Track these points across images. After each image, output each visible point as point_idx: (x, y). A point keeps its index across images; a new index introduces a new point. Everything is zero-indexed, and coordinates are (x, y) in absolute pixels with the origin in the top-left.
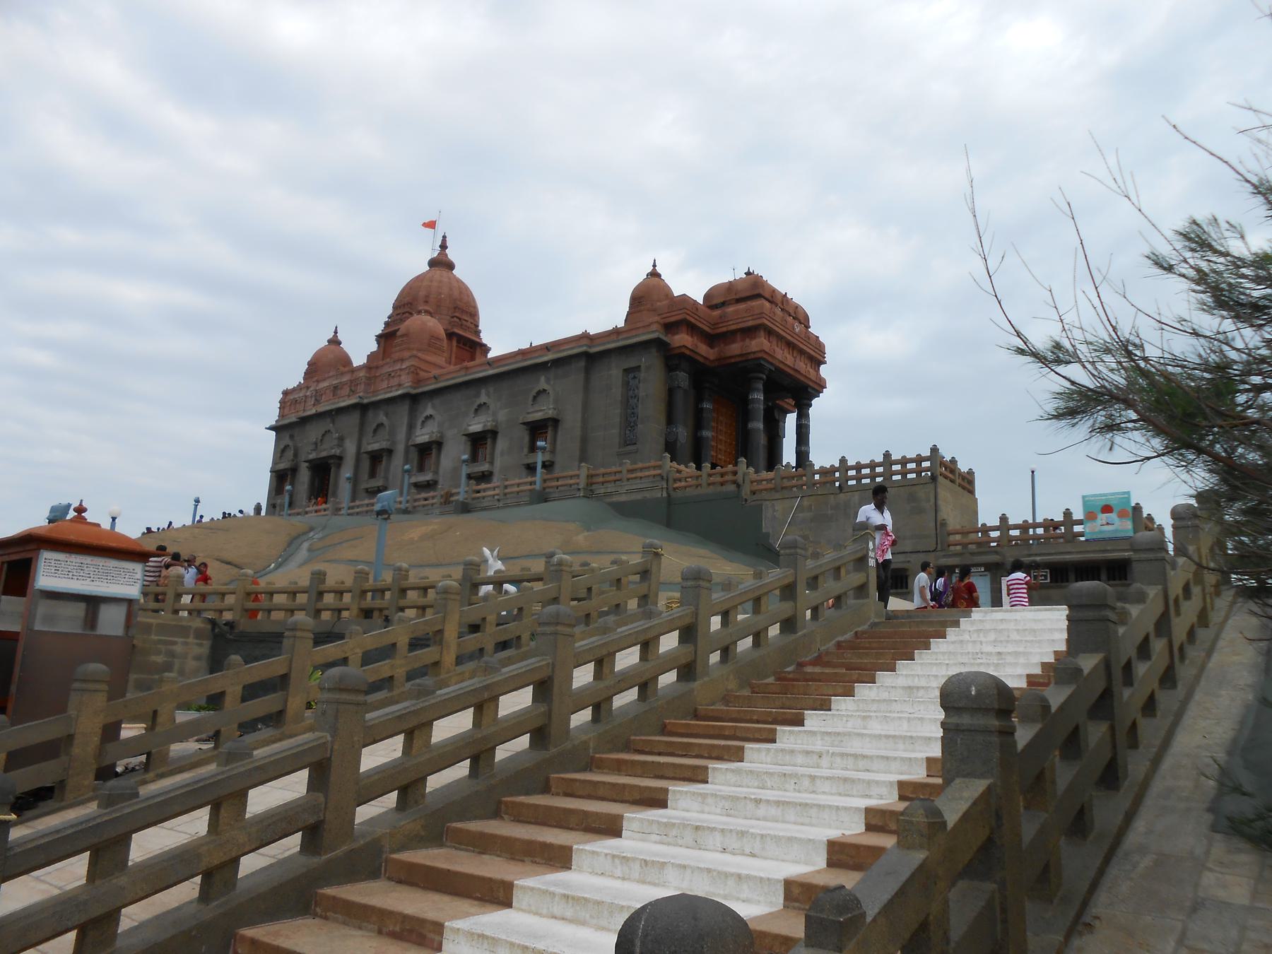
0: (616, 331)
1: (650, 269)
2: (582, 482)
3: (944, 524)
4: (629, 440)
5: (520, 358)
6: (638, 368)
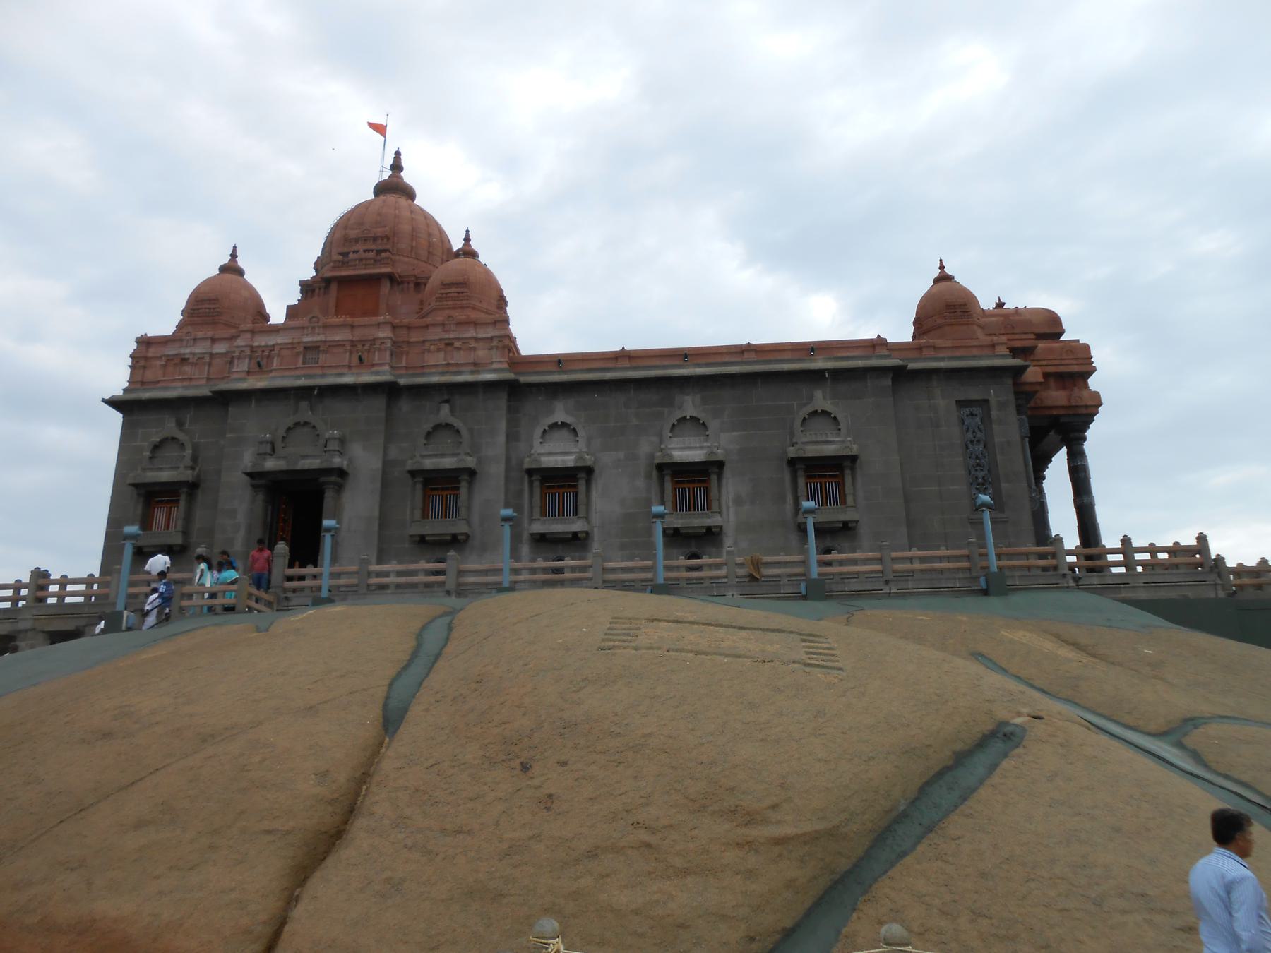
5: (753, 357)
6: (985, 403)
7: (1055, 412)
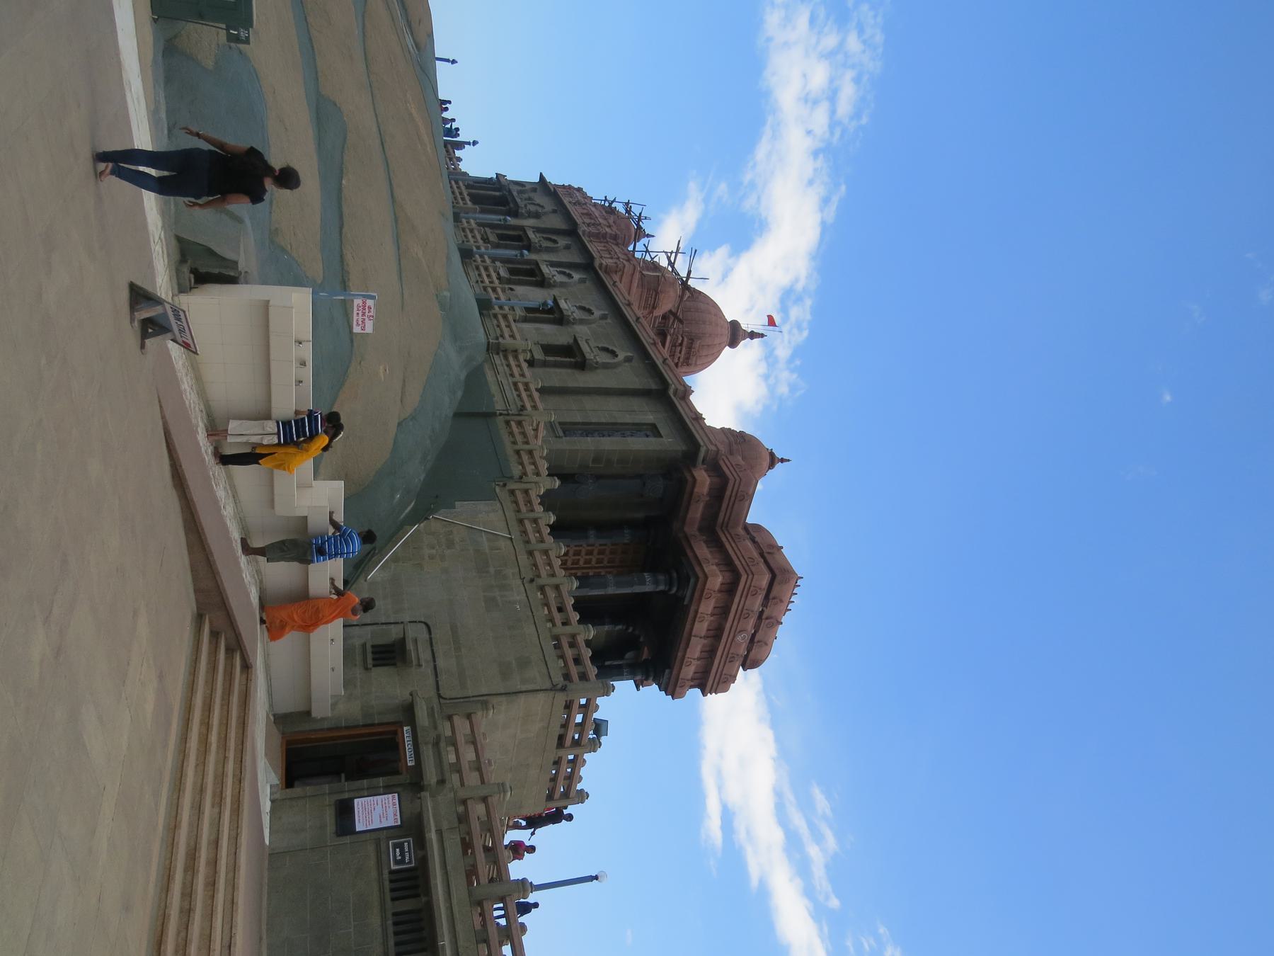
0: (698, 418)
1: (779, 455)
2: (507, 341)
3: (485, 705)
4: (569, 429)
6: (658, 435)
7: (688, 551)
